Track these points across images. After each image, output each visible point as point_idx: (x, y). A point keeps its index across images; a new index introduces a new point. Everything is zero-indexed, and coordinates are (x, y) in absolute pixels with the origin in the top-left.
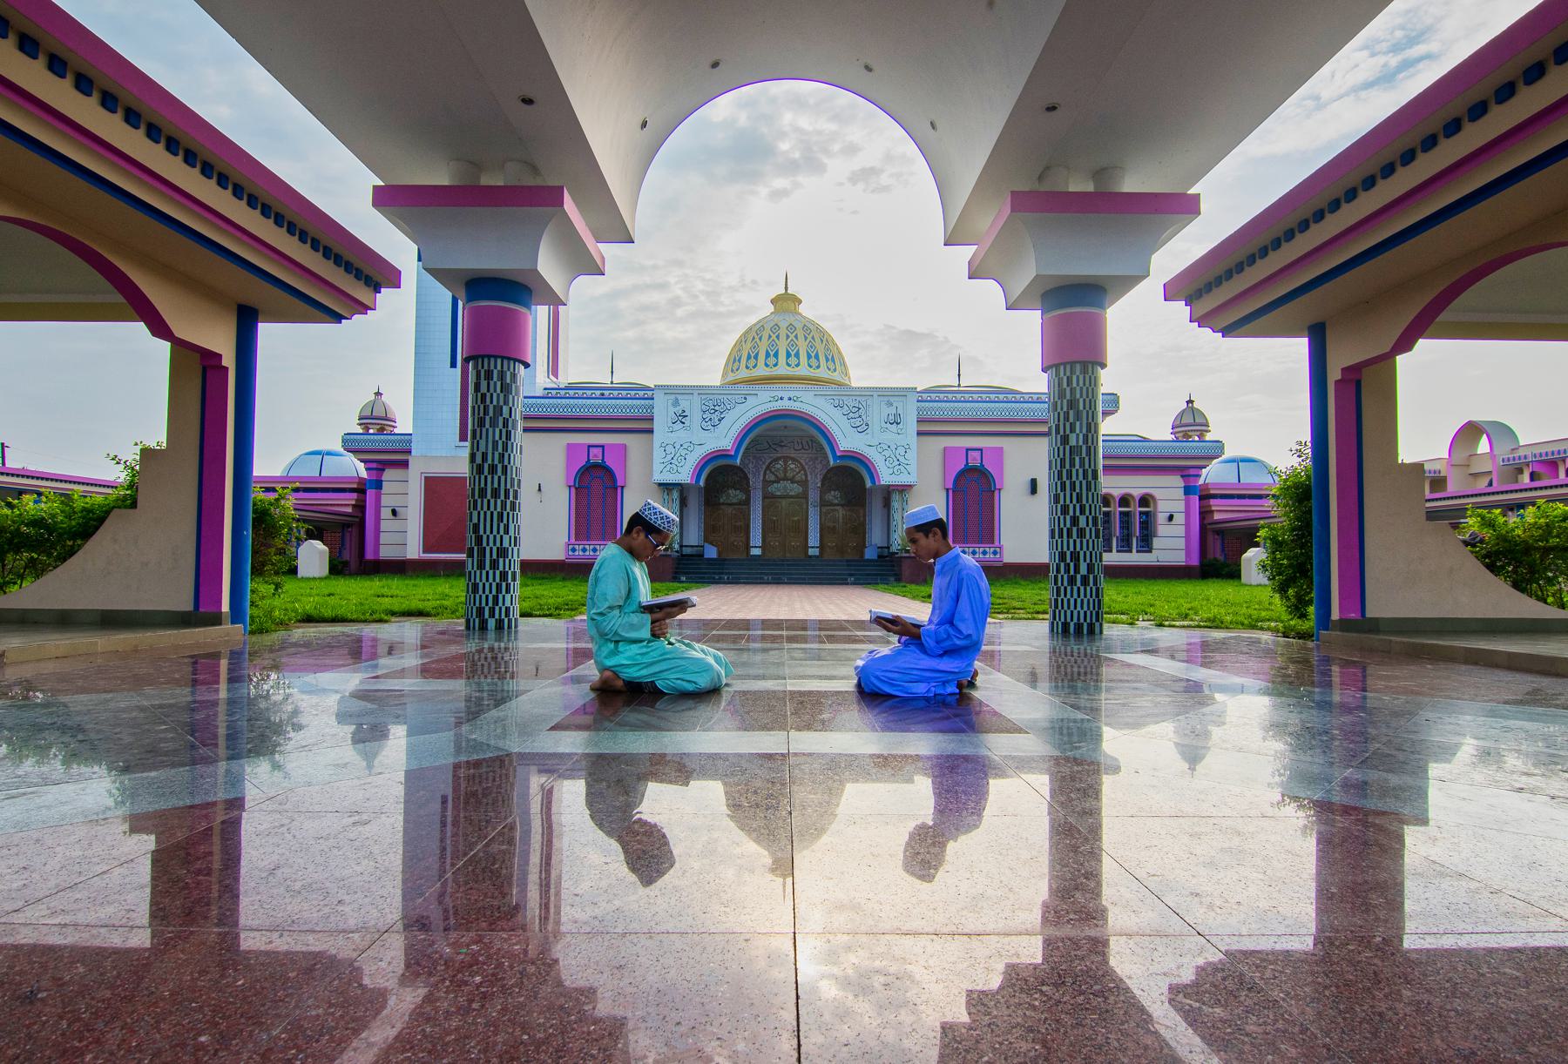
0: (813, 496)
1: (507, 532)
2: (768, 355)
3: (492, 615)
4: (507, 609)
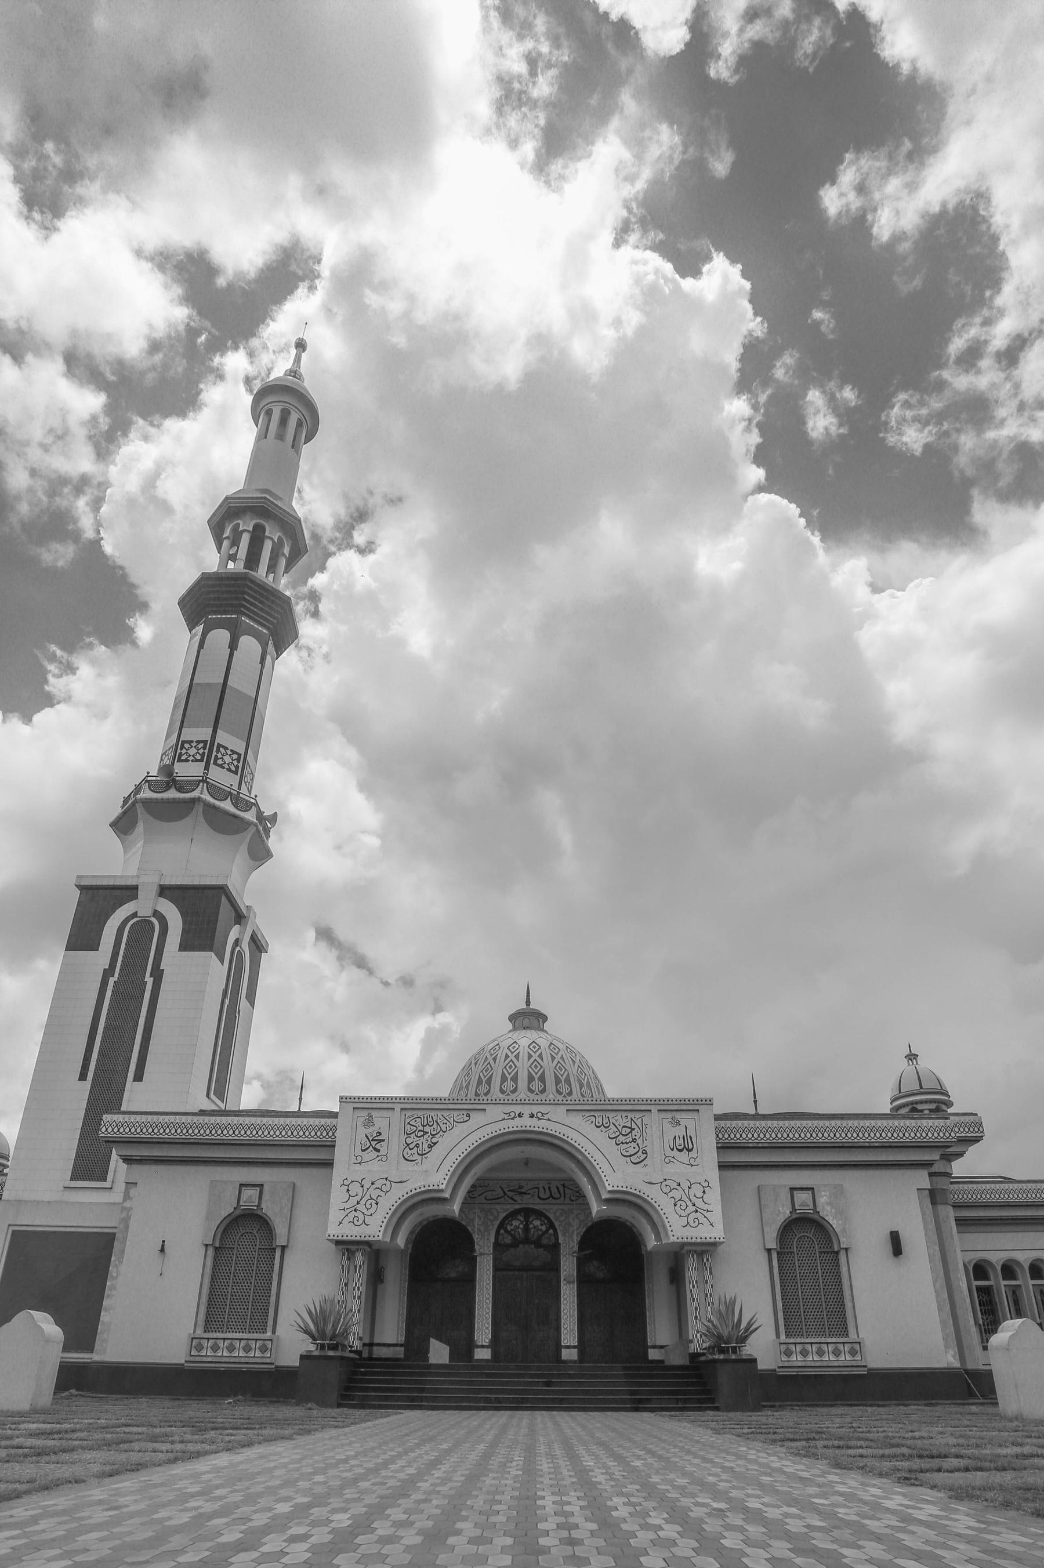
2: (504, 1079)
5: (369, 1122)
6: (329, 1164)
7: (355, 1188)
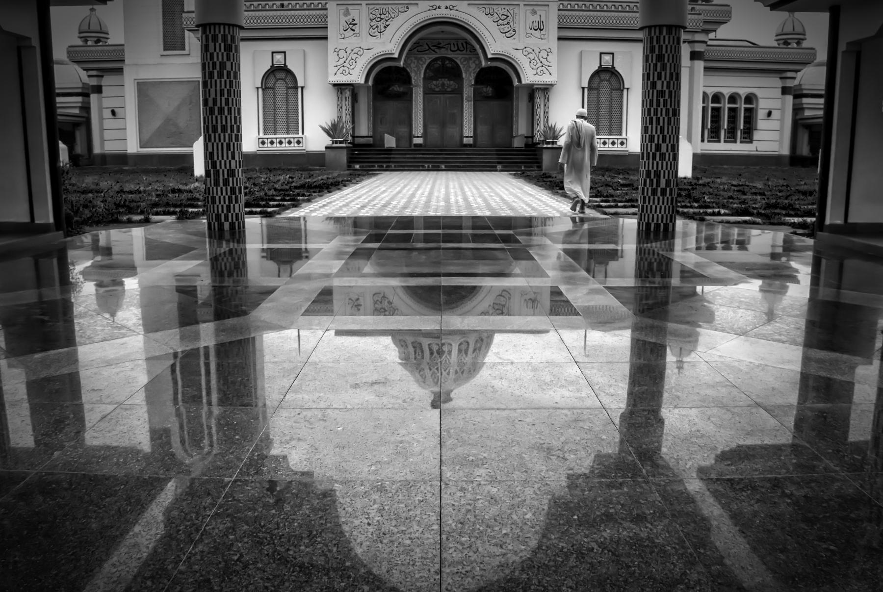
0: (468, 91)
1: (233, 158)
3: (226, 219)
4: (237, 214)
5: (347, 13)
6: (326, 38)
7: (342, 53)
